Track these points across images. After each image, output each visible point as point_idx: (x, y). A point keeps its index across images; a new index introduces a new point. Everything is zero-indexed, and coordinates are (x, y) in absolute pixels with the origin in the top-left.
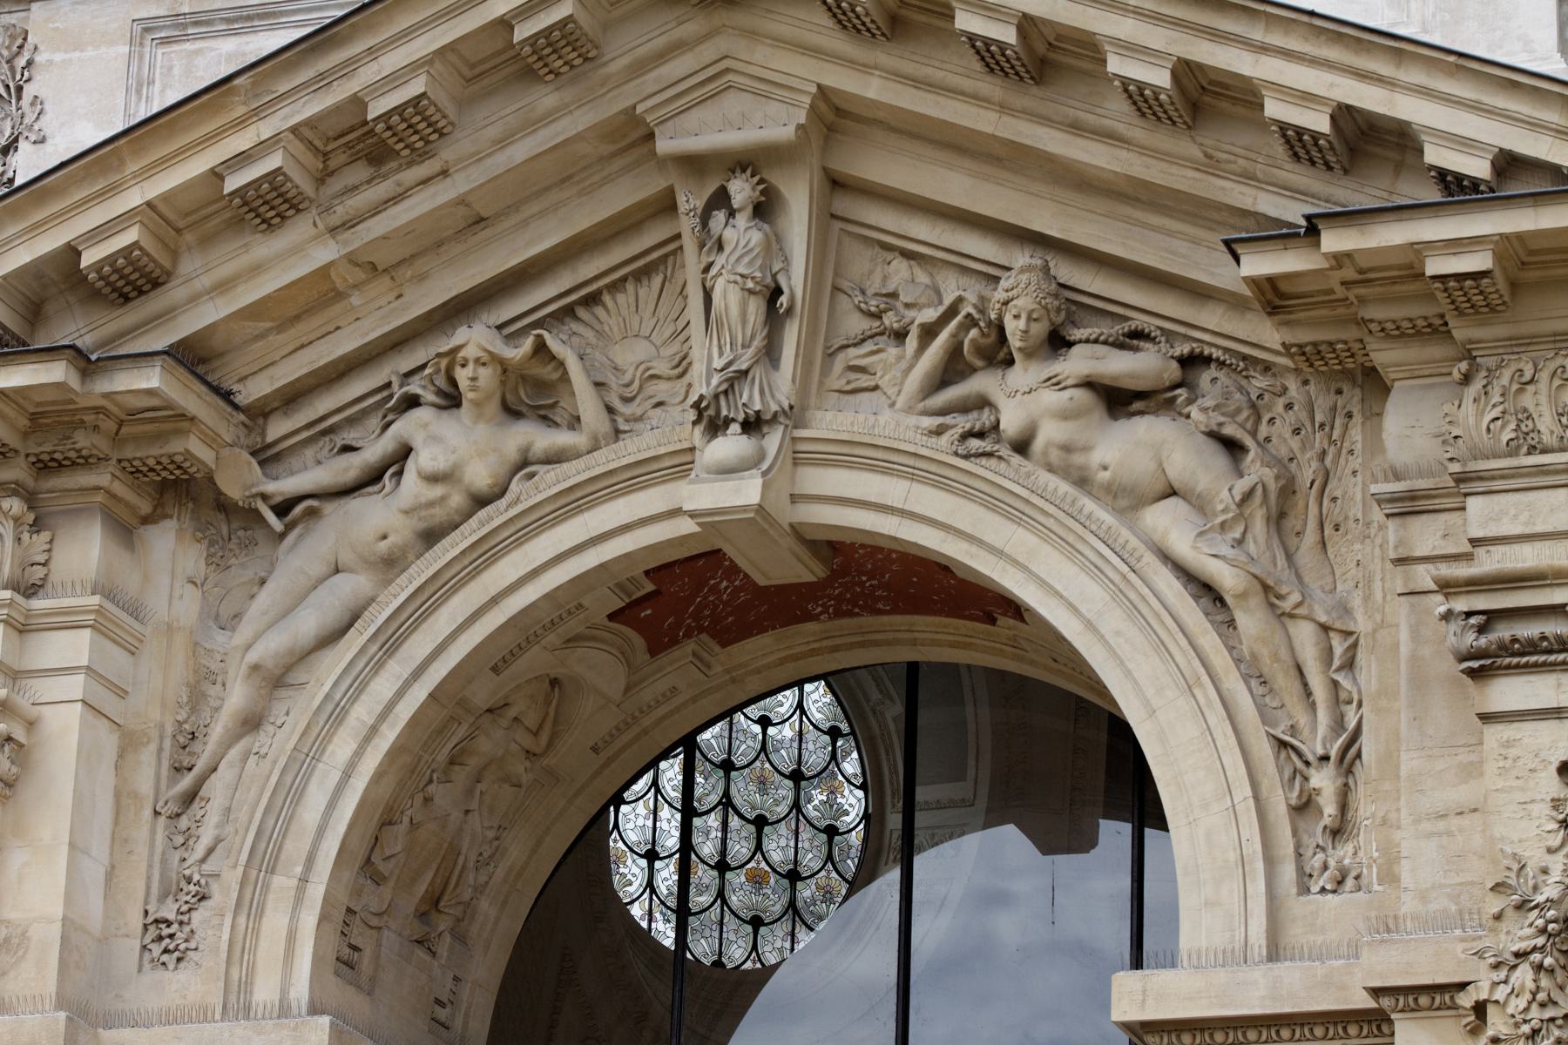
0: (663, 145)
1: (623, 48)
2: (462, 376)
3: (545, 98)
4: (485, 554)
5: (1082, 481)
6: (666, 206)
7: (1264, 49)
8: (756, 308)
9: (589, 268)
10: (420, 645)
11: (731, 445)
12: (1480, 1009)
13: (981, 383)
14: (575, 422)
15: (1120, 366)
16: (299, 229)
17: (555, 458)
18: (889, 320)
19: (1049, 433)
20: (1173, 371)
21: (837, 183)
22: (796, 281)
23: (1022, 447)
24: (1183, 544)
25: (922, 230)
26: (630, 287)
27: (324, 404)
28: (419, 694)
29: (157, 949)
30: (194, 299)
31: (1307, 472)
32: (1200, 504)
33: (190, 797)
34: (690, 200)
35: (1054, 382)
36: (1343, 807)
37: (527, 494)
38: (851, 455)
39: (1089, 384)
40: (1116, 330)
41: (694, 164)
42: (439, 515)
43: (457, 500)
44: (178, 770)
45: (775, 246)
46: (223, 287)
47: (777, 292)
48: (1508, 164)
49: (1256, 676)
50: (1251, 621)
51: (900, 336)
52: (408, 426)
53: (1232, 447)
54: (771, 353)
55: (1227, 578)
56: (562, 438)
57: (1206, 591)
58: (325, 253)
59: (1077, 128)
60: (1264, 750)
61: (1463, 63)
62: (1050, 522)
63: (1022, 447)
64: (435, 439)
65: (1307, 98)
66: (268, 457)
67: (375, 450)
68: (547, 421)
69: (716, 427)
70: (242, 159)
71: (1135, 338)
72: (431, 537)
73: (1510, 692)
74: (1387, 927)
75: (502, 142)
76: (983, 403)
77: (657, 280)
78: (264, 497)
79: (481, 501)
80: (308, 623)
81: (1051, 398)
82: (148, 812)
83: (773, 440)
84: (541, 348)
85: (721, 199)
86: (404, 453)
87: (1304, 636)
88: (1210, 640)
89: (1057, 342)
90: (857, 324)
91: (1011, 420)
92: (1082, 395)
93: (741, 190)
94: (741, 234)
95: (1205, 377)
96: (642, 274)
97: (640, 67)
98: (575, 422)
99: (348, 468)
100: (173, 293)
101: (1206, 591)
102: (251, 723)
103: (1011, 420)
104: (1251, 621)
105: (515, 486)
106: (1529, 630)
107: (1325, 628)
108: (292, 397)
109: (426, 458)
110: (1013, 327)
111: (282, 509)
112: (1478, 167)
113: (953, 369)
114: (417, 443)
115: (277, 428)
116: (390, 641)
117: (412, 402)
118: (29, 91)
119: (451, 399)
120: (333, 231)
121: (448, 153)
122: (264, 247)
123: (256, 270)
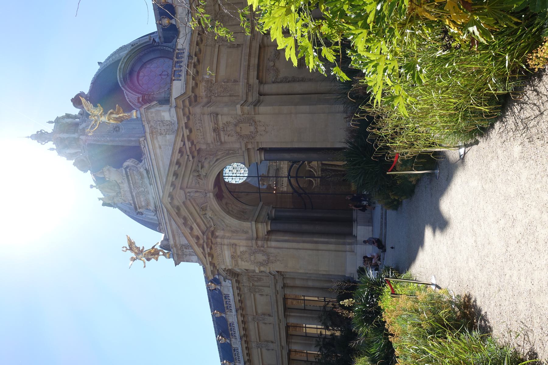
2: (203, 214)
7: (174, 159)
8: (197, 193)
9: (195, 205)
14: (207, 205)
16: (193, 226)
20: (200, 163)
24: (214, 162)
27: (206, 223)
30: (199, 233)
33: (236, 231)
36: (233, 151)
39: (201, 169)
44: (234, 232)
46: (198, 231)
48: (182, 141)
49: (223, 157)
55: (215, 159)
58: (195, 224)
60: (228, 157)
61: (174, 144)
63: (206, 174)
64: (209, 215)
66: (211, 227)
67: (210, 219)
69: (206, 195)
71: (198, 166)
72: (216, 215)
73: (223, 140)
74: (241, 148)
81: (203, 171)
86: (210, 217)
88: (220, 160)
89: (198, 171)
92: (202, 169)
95: (200, 160)
99: (211, 221)
100: (199, 235)
106: (218, 138)
109: (210, 216)
110: (197, 175)
111: (214, 225)
112: (182, 143)
115: (208, 226)
117: (206, 217)
121: (186, 216)
123: (196, 229)
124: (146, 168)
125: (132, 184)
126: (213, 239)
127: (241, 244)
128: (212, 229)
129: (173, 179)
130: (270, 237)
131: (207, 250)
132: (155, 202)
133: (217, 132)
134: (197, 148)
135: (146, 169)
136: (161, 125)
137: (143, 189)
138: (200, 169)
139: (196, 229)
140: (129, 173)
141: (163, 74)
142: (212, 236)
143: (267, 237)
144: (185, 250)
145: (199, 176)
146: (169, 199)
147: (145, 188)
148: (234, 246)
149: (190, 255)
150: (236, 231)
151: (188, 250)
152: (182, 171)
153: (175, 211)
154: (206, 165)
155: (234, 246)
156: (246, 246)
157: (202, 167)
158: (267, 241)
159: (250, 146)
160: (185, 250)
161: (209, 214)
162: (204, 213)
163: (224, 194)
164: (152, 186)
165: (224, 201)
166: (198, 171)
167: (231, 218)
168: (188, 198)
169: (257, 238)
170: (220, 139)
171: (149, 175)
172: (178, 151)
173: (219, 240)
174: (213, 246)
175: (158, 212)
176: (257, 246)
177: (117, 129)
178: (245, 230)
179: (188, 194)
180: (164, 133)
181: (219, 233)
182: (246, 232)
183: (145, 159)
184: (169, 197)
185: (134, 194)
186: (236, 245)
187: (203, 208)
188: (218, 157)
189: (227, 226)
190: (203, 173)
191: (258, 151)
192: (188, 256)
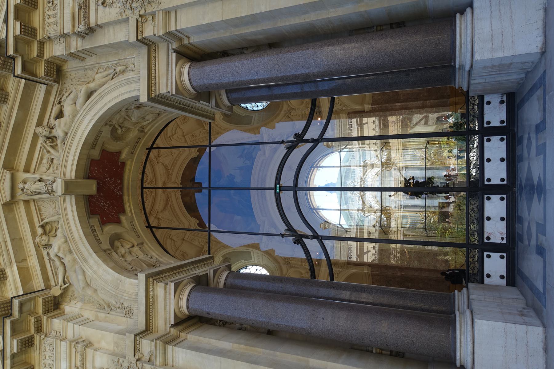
12: (141, 16)
16: (8, 272)
24: (80, 100)
26: (42, 213)
29: (130, 315)
33: (109, 306)
42: (67, 249)
62: (76, 126)
67: (58, 263)
72: (70, 252)
77: (42, 207)
78: (61, 286)
79: (66, 241)
80: (81, 277)
82: (108, 315)
88: (95, 94)
96: (40, 210)
102: (95, 291)
107: (97, 73)
120: (11, 265)
123: (15, 281)
126: (44, 318)
127: (103, 344)
128: (56, 291)
130: (183, 335)
134: (47, 55)
139: (15, 281)
142: (47, 311)
143: (173, 331)
145: (51, 139)
148: (80, 347)
150: (109, 306)
152: (10, 117)
154: (67, 110)
155: (80, 347)
156: (113, 354)
158: (168, 342)
159: (148, 32)
163: (123, 218)
165: (111, 229)
167: (100, 261)
168: (21, 197)
169: (147, 330)
170: (87, 16)
173: (57, 324)
174: (37, 338)
176: (137, 357)
179: (21, 186)
181: (69, 308)
182: (128, 313)
186: (88, 344)
187: (48, 228)
188: (92, 85)
189: (88, 285)
190: (59, 132)
191: (174, 54)
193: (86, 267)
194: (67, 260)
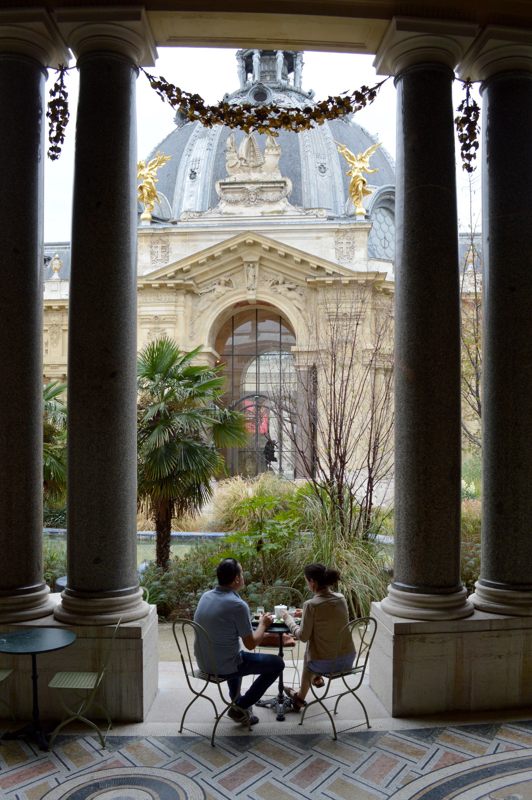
0: (244, 260)
1: (240, 250)
3: (232, 254)
4: (224, 300)
5: (286, 297)
6: (243, 265)
9: (233, 271)
10: (217, 309)
11: (251, 292)
13: (275, 286)
14: (233, 287)
15: (291, 286)
16: (205, 266)
17: (230, 291)
18: (266, 279)
19: (283, 292)
20: (295, 287)
21: (260, 264)
22: (257, 275)
23: (280, 293)
24: (297, 305)
25: (269, 270)
27: (205, 283)
28: (217, 315)
31: (308, 298)
32: (298, 301)
34: (246, 266)
35: (284, 287)
37: (228, 294)
38: (262, 293)
40: (289, 282)
41: (246, 262)
43: (221, 295)
45: (255, 271)
46: (196, 272)
47: (255, 276)
48: (334, 273)
50: (304, 313)
51: (267, 281)
52: (215, 287)
53: (301, 295)
54: (254, 282)
55: (302, 308)
56: (231, 289)
57: (299, 309)
58: (207, 269)
59: (288, 263)
63: (280, 293)
65: (314, 264)
68: (229, 286)
69: (249, 289)
70: (201, 260)
72: (218, 298)
75: (227, 258)
76: (275, 288)
79: (223, 295)
80: (205, 307)
83: (255, 291)
84: (230, 280)
85: (249, 266)
86: (214, 289)
87: (309, 314)
89: (284, 283)
90: (262, 279)
91: (279, 291)
93: (251, 265)
94: (251, 270)
95: (298, 287)
97: (242, 252)
98: (233, 287)
99: (208, 290)
101: (299, 309)
102: (199, 316)
103: (279, 291)
104: (304, 313)
105: (227, 293)
108: (201, 283)
112: (331, 273)
113: (273, 285)
114: (216, 288)
115: (200, 286)
116: (214, 309)
117: (215, 284)
118: (170, 247)
119: (220, 284)
121: (221, 259)
122: (201, 268)
123: (200, 270)
124: (286, 212)
125: (261, 186)
129: (282, 252)
131: (171, 283)
132: (234, 214)
133: (343, 317)
135: (284, 211)
136: (348, 246)
137: (254, 200)
138: (287, 285)
140: (279, 185)
141: (387, 242)
144: (160, 245)
145: (277, 283)
146: (252, 242)
147: (256, 203)
149: (152, 253)
151: (159, 250)
153: (232, 246)
154: (292, 294)
157: (290, 289)
160: (160, 245)
161: (220, 289)
162: (223, 282)
164: (260, 215)
166: (284, 283)
171: (276, 214)
172: (321, 265)
175: (220, 215)
177: (323, 170)
178: (195, 336)
180: (337, 248)
183: (299, 214)
184: (254, 241)
185: (247, 186)
190: (281, 288)
192: (150, 249)
193: (210, 309)
194: (212, 296)
